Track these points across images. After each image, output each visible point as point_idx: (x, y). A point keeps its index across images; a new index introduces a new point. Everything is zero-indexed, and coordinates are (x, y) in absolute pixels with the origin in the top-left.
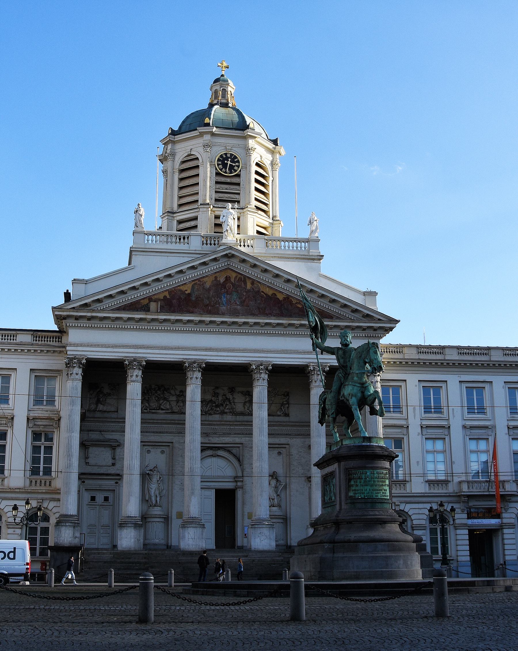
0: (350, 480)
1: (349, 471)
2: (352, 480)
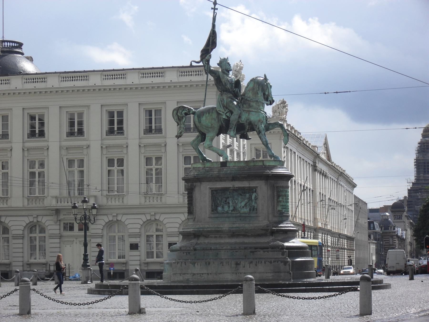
0: (279, 196)
1: (278, 189)
2: (281, 197)
